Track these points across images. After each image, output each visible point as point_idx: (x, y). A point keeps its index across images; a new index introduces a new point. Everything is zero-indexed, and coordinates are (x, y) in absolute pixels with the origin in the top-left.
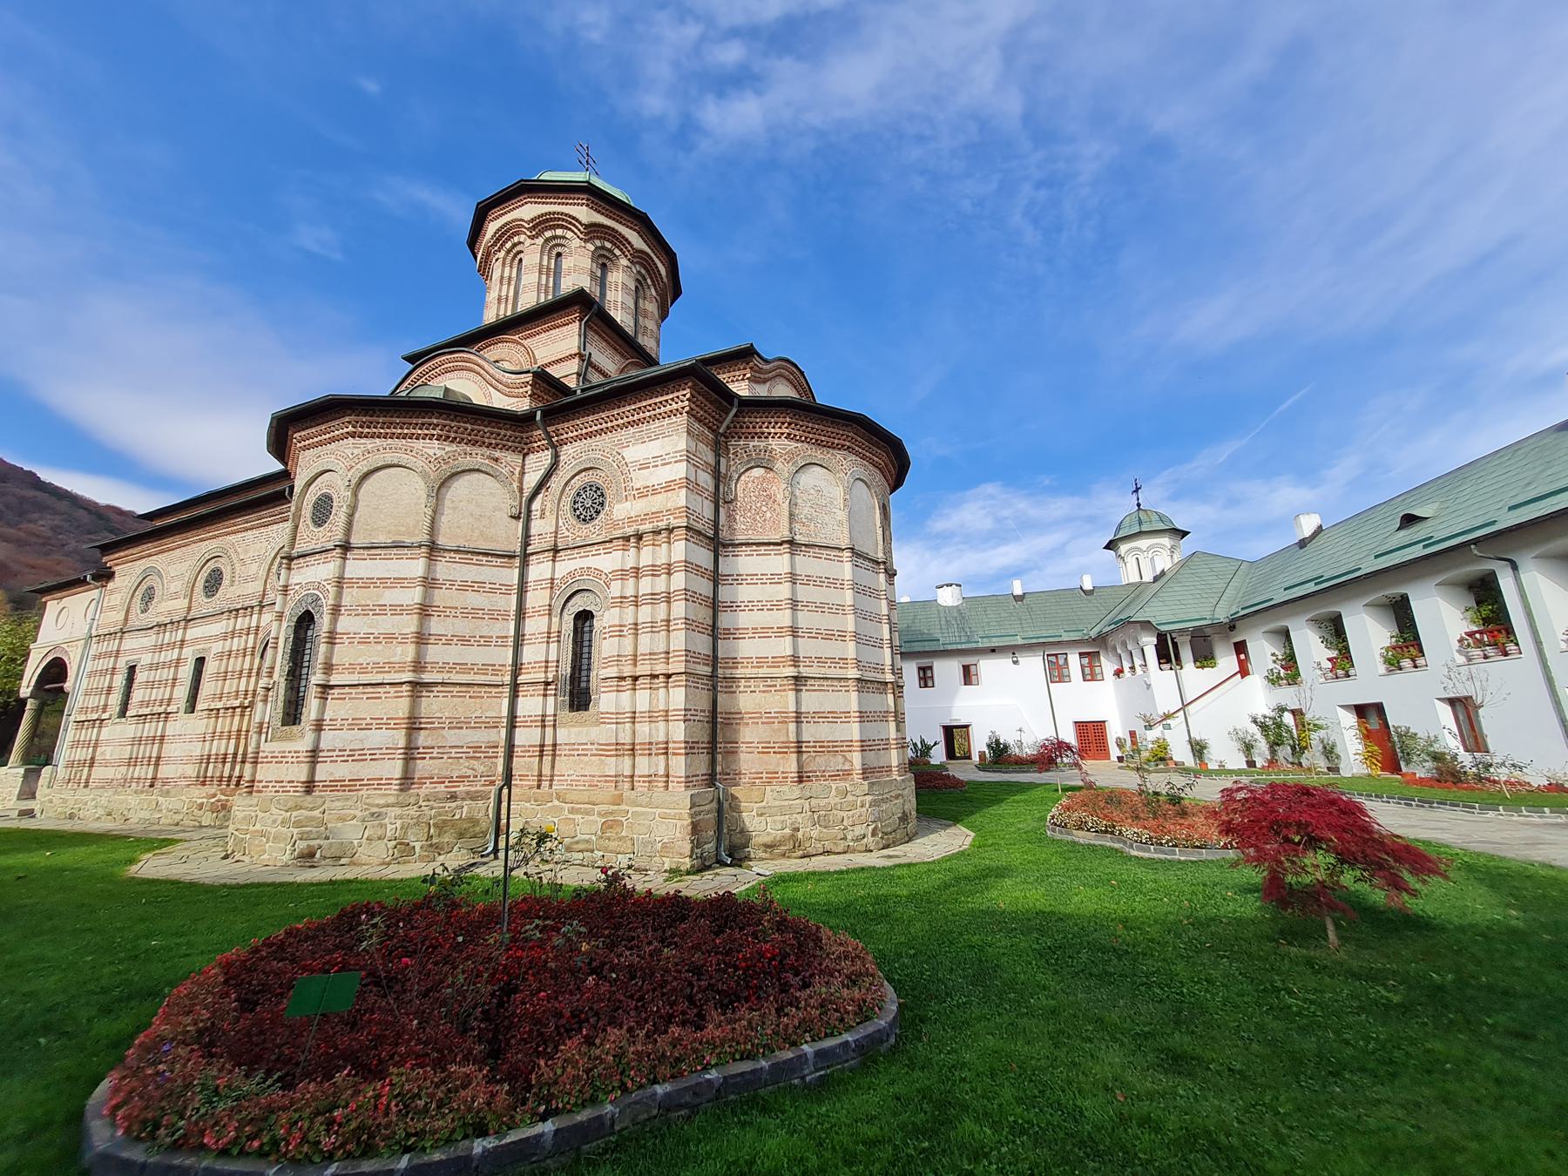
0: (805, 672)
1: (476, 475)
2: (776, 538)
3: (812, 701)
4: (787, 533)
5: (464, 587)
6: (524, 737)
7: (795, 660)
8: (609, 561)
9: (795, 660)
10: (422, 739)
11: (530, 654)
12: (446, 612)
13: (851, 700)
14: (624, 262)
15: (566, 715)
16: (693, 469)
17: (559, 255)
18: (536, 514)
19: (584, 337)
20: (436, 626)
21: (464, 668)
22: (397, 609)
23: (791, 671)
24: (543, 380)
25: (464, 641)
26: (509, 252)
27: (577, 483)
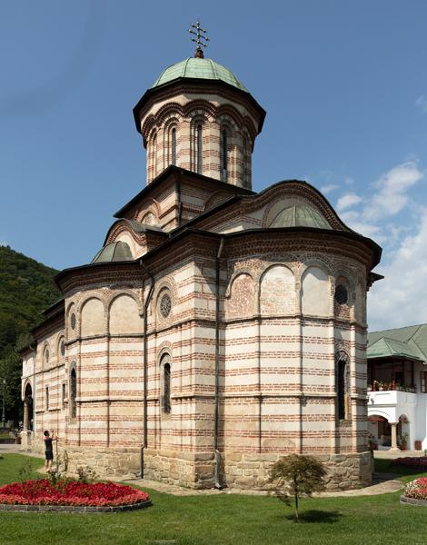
0: (264, 393)
1: (126, 297)
2: (250, 316)
3: (268, 409)
4: (257, 313)
5: (124, 354)
6: (151, 425)
7: (259, 386)
8: (174, 337)
9: (259, 386)
10: (112, 425)
11: (151, 385)
12: (116, 367)
13: (294, 408)
14: (211, 119)
15: (165, 415)
16: (200, 286)
17: (174, 130)
18: (149, 313)
19: (179, 192)
20: (113, 374)
21: (127, 393)
22: (100, 367)
23: (256, 393)
24: (151, 236)
25: (126, 380)
26: (152, 135)
27: (162, 295)
